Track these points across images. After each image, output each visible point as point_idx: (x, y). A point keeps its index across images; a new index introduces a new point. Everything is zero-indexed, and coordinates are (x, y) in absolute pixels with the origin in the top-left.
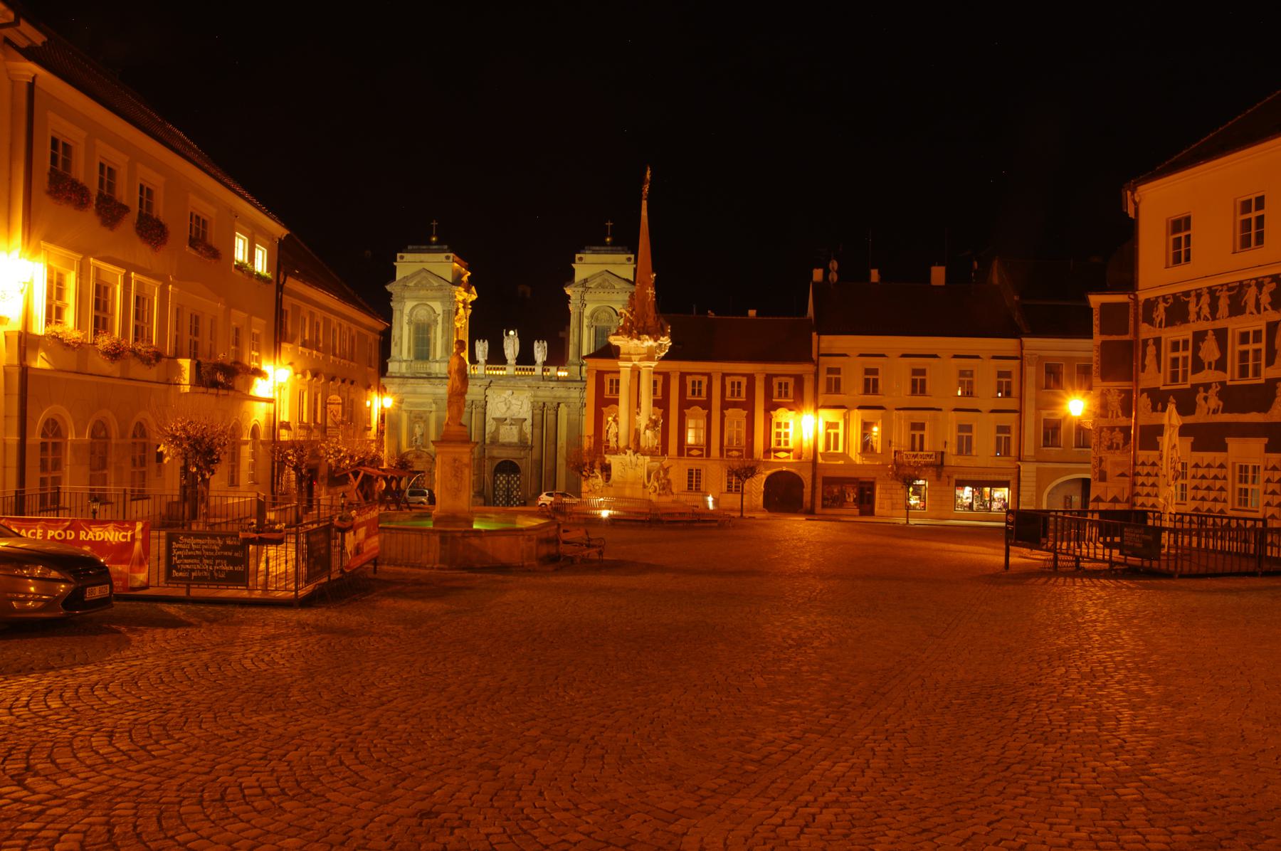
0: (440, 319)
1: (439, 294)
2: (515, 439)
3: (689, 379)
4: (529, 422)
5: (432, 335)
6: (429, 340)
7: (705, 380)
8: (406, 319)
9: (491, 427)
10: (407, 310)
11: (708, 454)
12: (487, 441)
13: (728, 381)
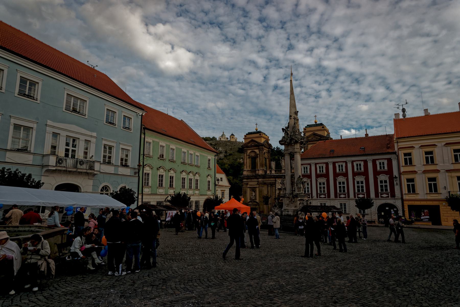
3: (337, 165)
7: (344, 165)
8: (248, 157)
9: (277, 192)
10: (248, 154)
11: (349, 197)
13: (355, 164)
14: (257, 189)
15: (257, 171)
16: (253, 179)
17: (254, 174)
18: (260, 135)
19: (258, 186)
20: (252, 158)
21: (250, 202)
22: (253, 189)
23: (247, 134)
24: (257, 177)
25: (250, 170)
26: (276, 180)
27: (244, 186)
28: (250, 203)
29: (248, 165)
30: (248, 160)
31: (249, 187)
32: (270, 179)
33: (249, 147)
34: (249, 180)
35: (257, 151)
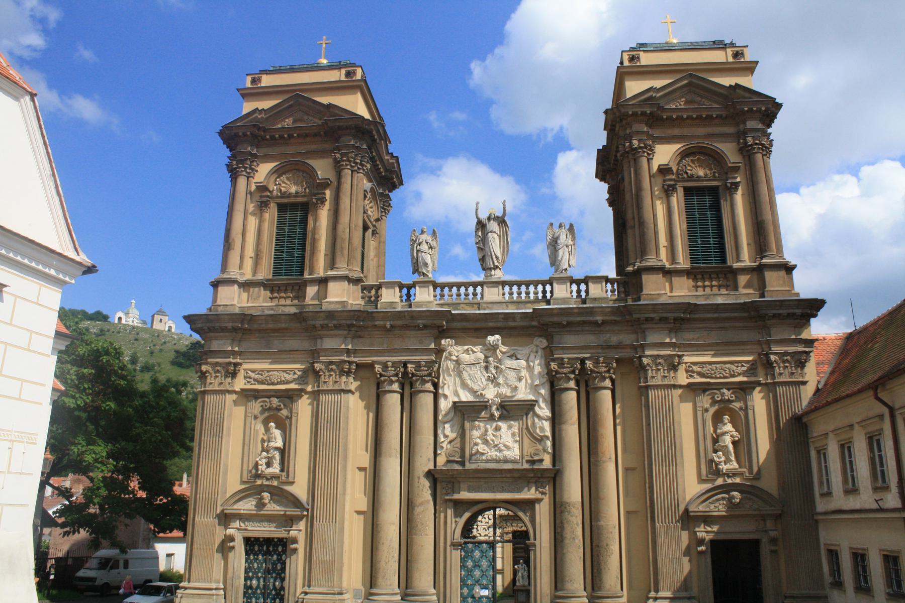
2: (514, 452)
4: (544, 410)
12: (441, 460)
15: (311, 291)
17: (287, 306)
20: (282, 208)
21: (242, 496)
22: (276, 407)
26: (439, 352)
28: (247, 506)
29: (250, 251)
32: (398, 344)
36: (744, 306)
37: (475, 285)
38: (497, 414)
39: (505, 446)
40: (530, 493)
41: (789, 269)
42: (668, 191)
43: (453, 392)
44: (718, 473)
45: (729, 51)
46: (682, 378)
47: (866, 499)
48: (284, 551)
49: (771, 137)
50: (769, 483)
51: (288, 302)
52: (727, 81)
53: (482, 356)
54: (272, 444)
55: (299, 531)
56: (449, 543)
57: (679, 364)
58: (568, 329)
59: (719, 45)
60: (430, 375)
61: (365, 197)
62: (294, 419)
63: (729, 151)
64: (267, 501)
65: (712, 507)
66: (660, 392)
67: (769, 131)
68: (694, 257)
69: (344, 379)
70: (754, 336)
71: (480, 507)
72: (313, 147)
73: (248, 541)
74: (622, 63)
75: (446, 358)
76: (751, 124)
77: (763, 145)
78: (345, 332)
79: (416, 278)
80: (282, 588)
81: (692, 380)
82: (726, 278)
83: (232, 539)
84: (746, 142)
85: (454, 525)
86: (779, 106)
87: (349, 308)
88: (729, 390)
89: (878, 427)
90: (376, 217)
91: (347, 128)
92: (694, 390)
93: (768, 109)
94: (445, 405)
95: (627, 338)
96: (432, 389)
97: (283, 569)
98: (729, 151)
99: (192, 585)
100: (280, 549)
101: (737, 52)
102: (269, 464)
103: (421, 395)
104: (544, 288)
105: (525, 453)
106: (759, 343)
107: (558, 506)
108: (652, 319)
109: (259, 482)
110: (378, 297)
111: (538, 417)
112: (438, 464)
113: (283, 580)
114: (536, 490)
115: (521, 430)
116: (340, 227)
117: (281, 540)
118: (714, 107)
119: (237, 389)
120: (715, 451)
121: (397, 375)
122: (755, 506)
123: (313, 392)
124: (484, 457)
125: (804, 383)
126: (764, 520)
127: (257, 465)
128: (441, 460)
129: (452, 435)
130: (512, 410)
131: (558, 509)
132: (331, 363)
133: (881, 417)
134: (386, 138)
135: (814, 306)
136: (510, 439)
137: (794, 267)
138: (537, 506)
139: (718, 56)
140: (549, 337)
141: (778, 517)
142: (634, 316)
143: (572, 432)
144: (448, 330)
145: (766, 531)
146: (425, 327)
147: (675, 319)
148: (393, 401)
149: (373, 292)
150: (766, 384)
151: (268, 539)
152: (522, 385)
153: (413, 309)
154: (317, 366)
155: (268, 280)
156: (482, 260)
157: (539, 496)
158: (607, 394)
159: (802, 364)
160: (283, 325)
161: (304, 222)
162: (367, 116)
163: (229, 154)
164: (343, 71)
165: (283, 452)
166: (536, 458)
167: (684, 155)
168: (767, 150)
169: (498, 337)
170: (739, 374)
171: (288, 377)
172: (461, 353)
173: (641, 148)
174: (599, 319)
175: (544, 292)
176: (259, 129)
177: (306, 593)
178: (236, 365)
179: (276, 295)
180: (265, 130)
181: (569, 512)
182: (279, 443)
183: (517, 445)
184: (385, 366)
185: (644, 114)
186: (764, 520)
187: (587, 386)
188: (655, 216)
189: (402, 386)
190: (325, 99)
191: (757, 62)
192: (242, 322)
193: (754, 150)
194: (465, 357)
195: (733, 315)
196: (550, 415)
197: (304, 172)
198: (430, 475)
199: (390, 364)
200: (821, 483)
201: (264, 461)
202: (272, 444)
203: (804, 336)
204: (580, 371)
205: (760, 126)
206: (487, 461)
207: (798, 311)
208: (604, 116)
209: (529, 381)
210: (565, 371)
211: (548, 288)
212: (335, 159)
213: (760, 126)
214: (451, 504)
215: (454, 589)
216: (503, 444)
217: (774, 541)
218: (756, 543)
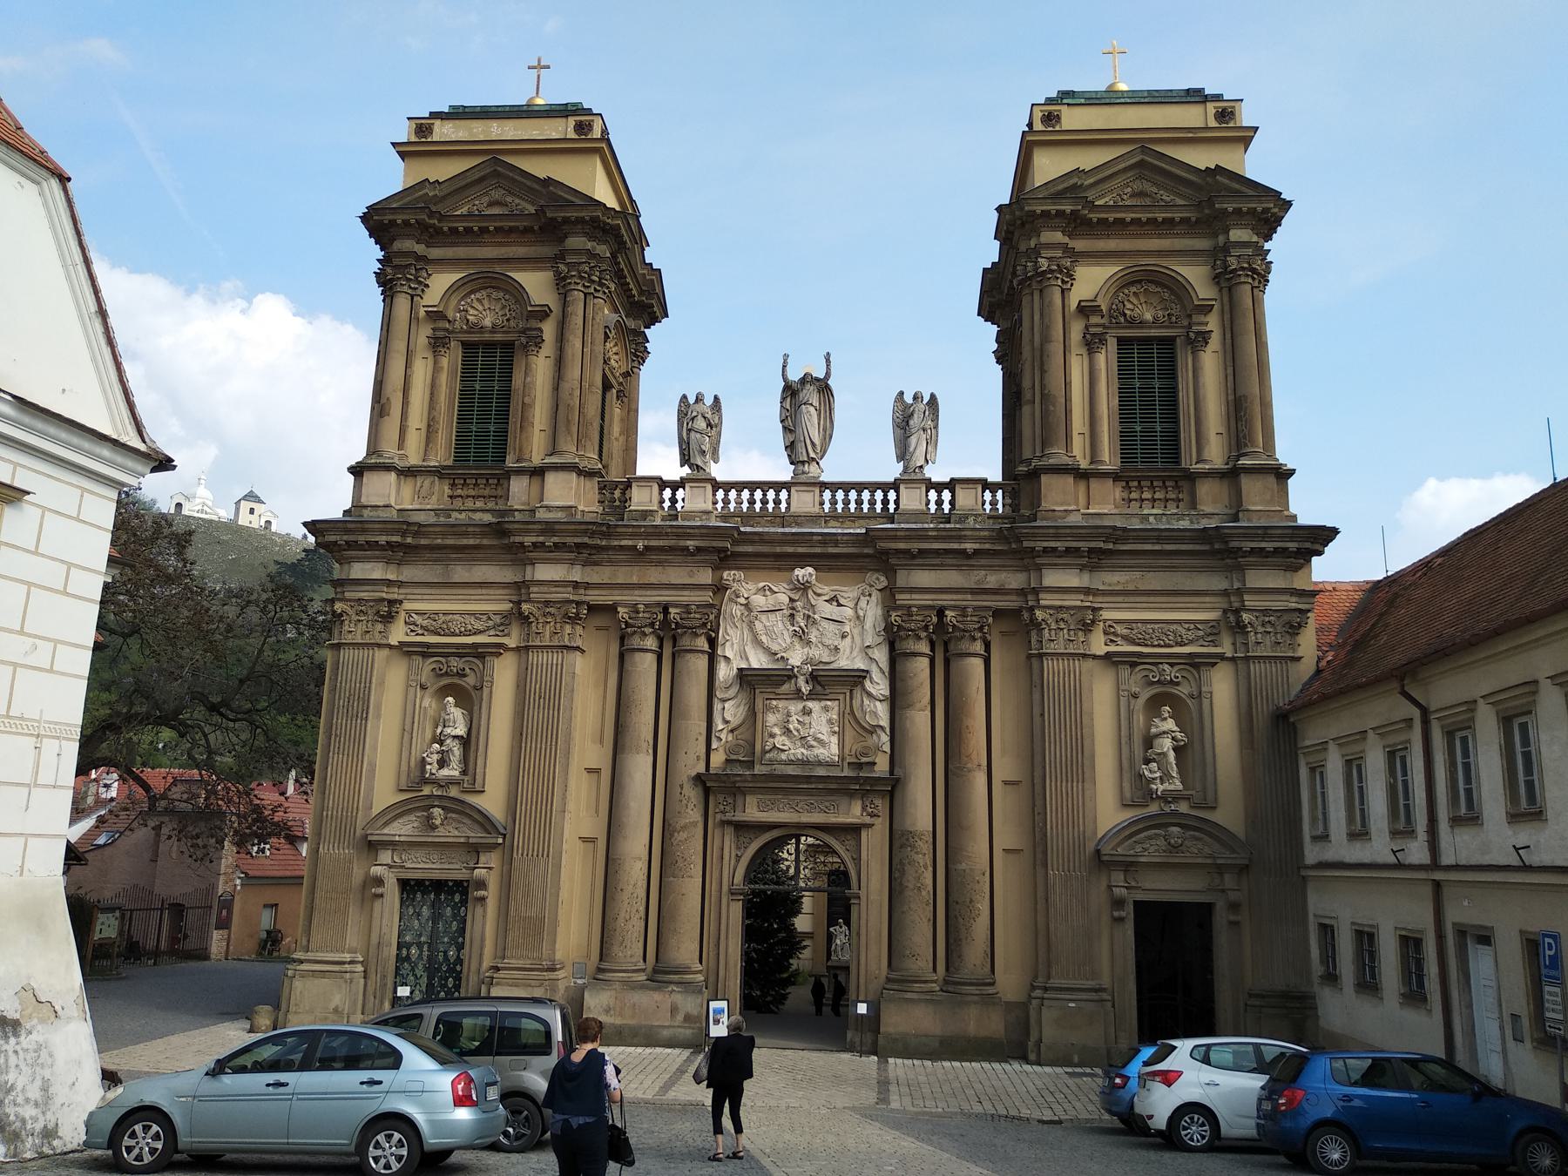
0: (548, 329)
1: (547, 251)
2: (831, 751)
4: (879, 685)
5: (517, 380)
6: (506, 395)
12: (717, 759)
14: (503, 676)
15: (519, 489)
16: (468, 553)
18: (582, 128)
19: (511, 642)
21: (395, 812)
22: (455, 672)
23: (435, 115)
24: (508, 540)
25: (439, 473)
26: (719, 588)
27: (353, 631)
29: (417, 419)
30: (421, 371)
31: (405, 650)
32: (654, 575)
33: (455, 236)
34: (409, 573)
35: (536, 284)
36: (1204, 535)
37: (778, 486)
38: (805, 689)
39: (816, 739)
40: (853, 812)
41: (1283, 475)
42: (1092, 343)
43: (740, 651)
44: (1150, 796)
45: (1211, 108)
46: (1098, 645)
47: (1379, 848)
48: (464, 902)
49: (1269, 258)
50: (1229, 814)
51: (479, 504)
52: (1200, 158)
53: (784, 599)
54: (448, 731)
55: (488, 869)
56: (725, 888)
57: (1093, 622)
58: (920, 561)
59: (1195, 96)
60: (704, 624)
61: (607, 337)
62: (486, 691)
63: (1196, 276)
64: (438, 822)
65: (1139, 849)
66: (1061, 665)
67: (1267, 246)
68: (1127, 453)
69: (568, 629)
70: (1218, 582)
71: (775, 833)
72: (521, 251)
73: (404, 884)
74: (1030, 125)
75: (731, 600)
76: (1237, 235)
77: (1254, 271)
78: (572, 556)
79: (686, 471)
80: (459, 961)
81: (1112, 648)
82: (1177, 487)
83: (379, 881)
84: (1225, 266)
85: (734, 863)
86: (1288, 205)
87: (579, 517)
88: (1172, 665)
89: (1403, 738)
90: (624, 370)
91: (580, 221)
92: (1116, 664)
93: (1268, 210)
94: (724, 672)
95: (1015, 580)
96: (706, 647)
97: (462, 931)
98: (1196, 276)
99: (310, 956)
100: (457, 898)
101: (1224, 109)
102: (442, 763)
103: (689, 656)
104: (885, 496)
105: (847, 751)
106: (1225, 593)
107: (896, 836)
108: (1054, 549)
109: (426, 790)
110: (625, 500)
111: (869, 695)
112: (712, 765)
113: (460, 947)
114: (864, 809)
115: (841, 715)
116: (565, 386)
117: (459, 883)
118: (1177, 204)
119: (394, 642)
120: (1147, 762)
121: (652, 625)
122: (1207, 850)
123: (518, 649)
124: (783, 756)
125: (1299, 659)
126: (1221, 874)
127: (423, 762)
128: (717, 759)
129: (735, 722)
130: (829, 683)
131: (898, 840)
132: (547, 603)
133: (1409, 722)
134: (640, 239)
135: (1322, 536)
136: (825, 729)
137: (1291, 472)
138: (864, 834)
139: (1191, 116)
140: (890, 572)
141: (1243, 870)
142: (1026, 544)
143: (919, 721)
144: (735, 555)
145: (1223, 891)
146: (699, 549)
147: (1091, 550)
148: (645, 664)
149: (617, 493)
150: (1233, 659)
151: (439, 881)
152: (845, 645)
153: (680, 522)
154: (525, 607)
155: (444, 468)
156: (790, 447)
157: (867, 820)
158: (977, 665)
159: (1294, 629)
160: (471, 542)
161: (507, 376)
162: (612, 202)
163: (380, 255)
164: (572, 121)
165: (466, 742)
166: (864, 760)
167: (1128, 282)
168: (1261, 277)
169: (810, 570)
170: (1191, 642)
171: (478, 625)
172: (757, 593)
173: (1052, 271)
174: (969, 546)
175: (885, 502)
176: (432, 214)
177: (497, 969)
178: (391, 602)
179: (459, 492)
180: (442, 218)
181: (913, 847)
182: (461, 730)
183: (834, 740)
184: (634, 608)
185: (1060, 214)
186: (1221, 874)
187: (946, 650)
188: (1068, 384)
189: (661, 640)
190: (539, 168)
191: (1257, 128)
192: (404, 535)
193: (1243, 276)
194: (759, 601)
195: (1184, 547)
196: (887, 693)
197: (506, 291)
198: (699, 779)
199: (641, 607)
200: (1314, 820)
201: (436, 757)
202: (448, 731)
203: (1298, 582)
204: (936, 626)
205: (1255, 239)
206: (790, 762)
207: (1292, 546)
208: (996, 215)
209: (858, 639)
210: (913, 626)
211: (892, 495)
212: (557, 273)
213: (1255, 239)
214: (729, 831)
215: (731, 963)
216: (812, 734)
217: (1234, 907)
218: (1207, 908)
